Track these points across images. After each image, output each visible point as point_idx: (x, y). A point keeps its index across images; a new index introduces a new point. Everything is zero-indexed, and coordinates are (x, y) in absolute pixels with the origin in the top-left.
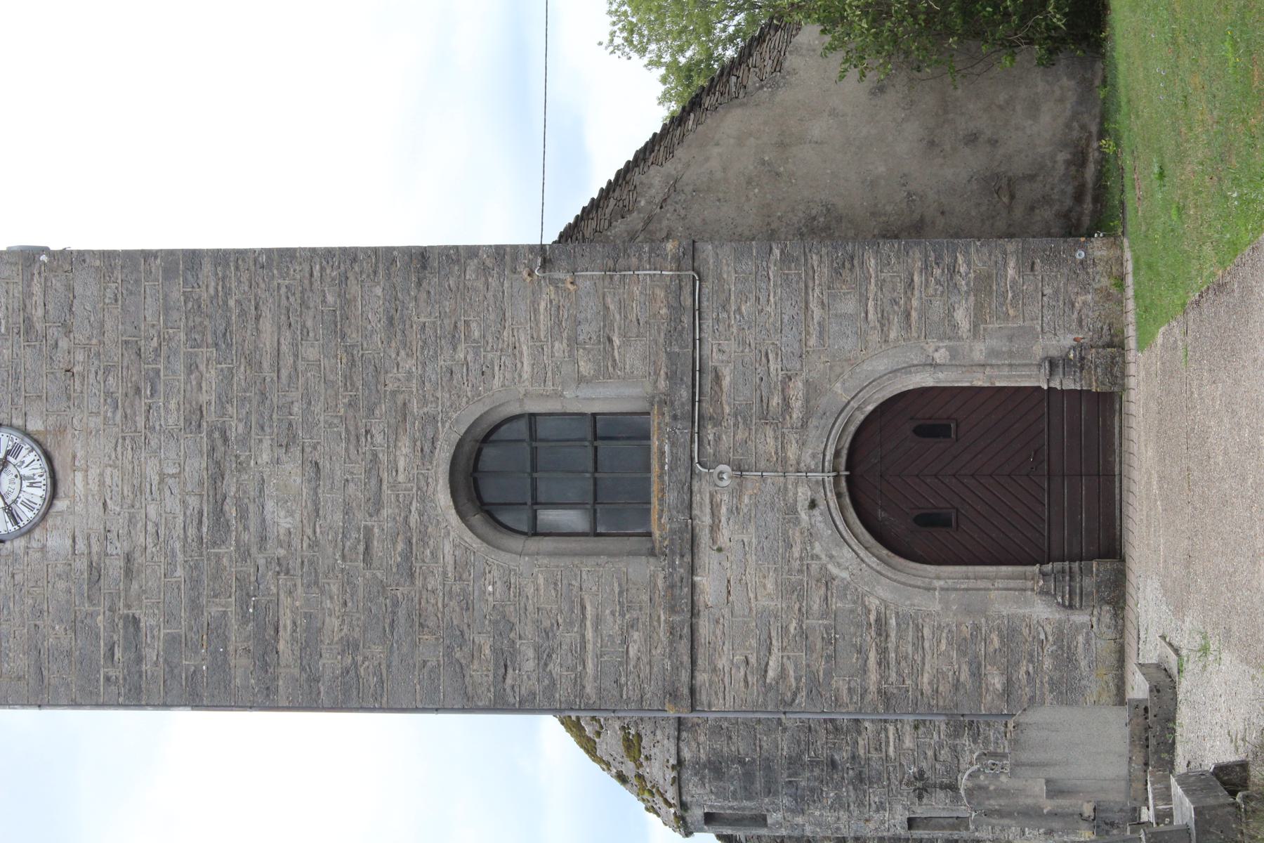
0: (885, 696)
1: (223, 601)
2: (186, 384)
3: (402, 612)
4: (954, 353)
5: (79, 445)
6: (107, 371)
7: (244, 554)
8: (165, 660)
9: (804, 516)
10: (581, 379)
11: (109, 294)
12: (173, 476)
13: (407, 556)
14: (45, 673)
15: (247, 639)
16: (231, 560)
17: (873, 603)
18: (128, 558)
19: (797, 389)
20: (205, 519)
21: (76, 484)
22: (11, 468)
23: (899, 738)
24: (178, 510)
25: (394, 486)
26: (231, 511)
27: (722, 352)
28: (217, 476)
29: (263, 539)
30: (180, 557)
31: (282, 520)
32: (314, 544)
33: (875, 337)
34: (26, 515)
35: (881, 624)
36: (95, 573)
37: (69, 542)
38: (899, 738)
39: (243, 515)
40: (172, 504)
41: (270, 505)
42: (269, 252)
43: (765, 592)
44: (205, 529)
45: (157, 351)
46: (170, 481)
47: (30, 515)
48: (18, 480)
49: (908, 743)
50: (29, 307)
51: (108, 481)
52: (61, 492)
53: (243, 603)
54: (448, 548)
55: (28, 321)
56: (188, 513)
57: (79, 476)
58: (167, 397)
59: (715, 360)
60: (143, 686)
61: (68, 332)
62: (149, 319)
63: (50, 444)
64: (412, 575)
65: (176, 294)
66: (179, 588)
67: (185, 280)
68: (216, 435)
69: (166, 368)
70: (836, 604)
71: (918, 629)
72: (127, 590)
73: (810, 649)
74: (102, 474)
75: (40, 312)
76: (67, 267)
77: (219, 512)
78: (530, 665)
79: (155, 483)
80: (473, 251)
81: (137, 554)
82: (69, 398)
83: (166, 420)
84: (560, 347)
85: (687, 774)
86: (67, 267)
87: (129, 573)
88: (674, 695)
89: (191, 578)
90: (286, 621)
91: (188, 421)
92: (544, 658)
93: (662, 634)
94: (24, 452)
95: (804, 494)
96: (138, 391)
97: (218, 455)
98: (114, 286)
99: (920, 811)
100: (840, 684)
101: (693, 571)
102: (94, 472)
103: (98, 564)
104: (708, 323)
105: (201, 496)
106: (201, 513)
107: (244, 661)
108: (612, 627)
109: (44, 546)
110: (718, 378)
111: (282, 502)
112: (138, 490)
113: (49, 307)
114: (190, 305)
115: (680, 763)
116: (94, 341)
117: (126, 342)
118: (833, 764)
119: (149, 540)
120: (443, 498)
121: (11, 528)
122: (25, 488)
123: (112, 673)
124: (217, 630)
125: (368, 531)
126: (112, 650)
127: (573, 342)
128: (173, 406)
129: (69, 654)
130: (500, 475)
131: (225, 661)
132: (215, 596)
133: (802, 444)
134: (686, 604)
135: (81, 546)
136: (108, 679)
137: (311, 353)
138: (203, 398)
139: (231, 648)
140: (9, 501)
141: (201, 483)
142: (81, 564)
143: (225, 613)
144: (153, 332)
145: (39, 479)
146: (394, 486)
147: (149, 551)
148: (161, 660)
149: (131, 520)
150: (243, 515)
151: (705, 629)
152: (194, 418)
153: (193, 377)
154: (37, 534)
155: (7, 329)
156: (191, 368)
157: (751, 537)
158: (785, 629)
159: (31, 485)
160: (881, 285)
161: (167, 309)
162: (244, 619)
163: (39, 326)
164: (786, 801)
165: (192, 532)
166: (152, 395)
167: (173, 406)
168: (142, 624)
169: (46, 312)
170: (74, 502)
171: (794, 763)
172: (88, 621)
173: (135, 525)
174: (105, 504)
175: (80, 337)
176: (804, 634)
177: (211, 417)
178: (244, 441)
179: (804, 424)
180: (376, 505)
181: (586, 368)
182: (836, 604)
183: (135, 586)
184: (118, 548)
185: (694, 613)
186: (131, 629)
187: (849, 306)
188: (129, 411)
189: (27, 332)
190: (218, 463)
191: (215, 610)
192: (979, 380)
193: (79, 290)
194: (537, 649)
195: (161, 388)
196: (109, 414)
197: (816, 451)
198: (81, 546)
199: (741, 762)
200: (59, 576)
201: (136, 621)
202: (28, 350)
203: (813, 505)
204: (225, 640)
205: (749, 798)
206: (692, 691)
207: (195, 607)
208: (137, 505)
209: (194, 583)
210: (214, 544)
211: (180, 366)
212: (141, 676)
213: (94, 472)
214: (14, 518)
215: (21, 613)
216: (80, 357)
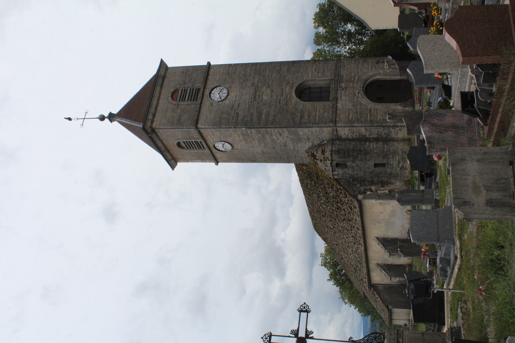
0: (371, 121)
3: (284, 111)
4: (384, 72)
7: (258, 103)
9: (357, 95)
10: (319, 77)
13: (286, 102)
17: (369, 107)
18: (239, 104)
19: (356, 77)
23: (373, 146)
25: (285, 93)
26: (257, 97)
27: (344, 73)
29: (262, 101)
31: (265, 98)
32: (271, 101)
33: (370, 70)
34: (223, 98)
35: (370, 110)
36: (233, 107)
38: (373, 146)
39: (259, 97)
40: (247, 97)
41: (264, 96)
42: (269, 62)
43: (350, 106)
49: (375, 146)
53: (257, 110)
54: (294, 101)
55: (229, 73)
59: (342, 73)
61: (234, 73)
64: (287, 105)
65: (253, 68)
70: (362, 107)
71: (377, 111)
73: (357, 114)
77: (255, 97)
78: (306, 118)
80: (303, 61)
84: (316, 73)
85: (333, 153)
87: (238, 106)
88: (332, 121)
90: (264, 112)
92: (309, 117)
93: (331, 112)
95: (357, 91)
99: (377, 162)
100: (363, 119)
101: (337, 103)
102: (235, 93)
104: (342, 69)
108: (322, 112)
110: (343, 76)
111: (266, 95)
112: (242, 95)
115: (332, 151)
118: (360, 150)
120: (294, 94)
124: (252, 114)
125: (280, 99)
127: (318, 72)
130: (304, 93)
133: (357, 85)
134: (335, 108)
135: (231, 103)
137: (274, 75)
142: (231, 105)
146: (285, 93)
150: (259, 97)
151: (338, 112)
152: (253, 84)
156: (254, 78)
157: (347, 98)
158: (353, 111)
160: (371, 63)
161: (251, 70)
162: (257, 112)
164: (351, 159)
171: (353, 150)
175: (236, 74)
176: (356, 112)
177: (256, 84)
178: (260, 87)
179: (358, 82)
180: (282, 95)
181: (320, 75)
182: (362, 107)
184: (237, 103)
185: (337, 109)
187: (366, 66)
191: (252, 111)
192: (388, 78)
194: (308, 115)
197: (358, 87)
198: (231, 103)
199: (343, 150)
201: (238, 113)
203: (359, 93)
205: (344, 158)
206: (336, 121)
207: (249, 111)
209: (249, 107)
211: (252, 78)
213: (235, 93)
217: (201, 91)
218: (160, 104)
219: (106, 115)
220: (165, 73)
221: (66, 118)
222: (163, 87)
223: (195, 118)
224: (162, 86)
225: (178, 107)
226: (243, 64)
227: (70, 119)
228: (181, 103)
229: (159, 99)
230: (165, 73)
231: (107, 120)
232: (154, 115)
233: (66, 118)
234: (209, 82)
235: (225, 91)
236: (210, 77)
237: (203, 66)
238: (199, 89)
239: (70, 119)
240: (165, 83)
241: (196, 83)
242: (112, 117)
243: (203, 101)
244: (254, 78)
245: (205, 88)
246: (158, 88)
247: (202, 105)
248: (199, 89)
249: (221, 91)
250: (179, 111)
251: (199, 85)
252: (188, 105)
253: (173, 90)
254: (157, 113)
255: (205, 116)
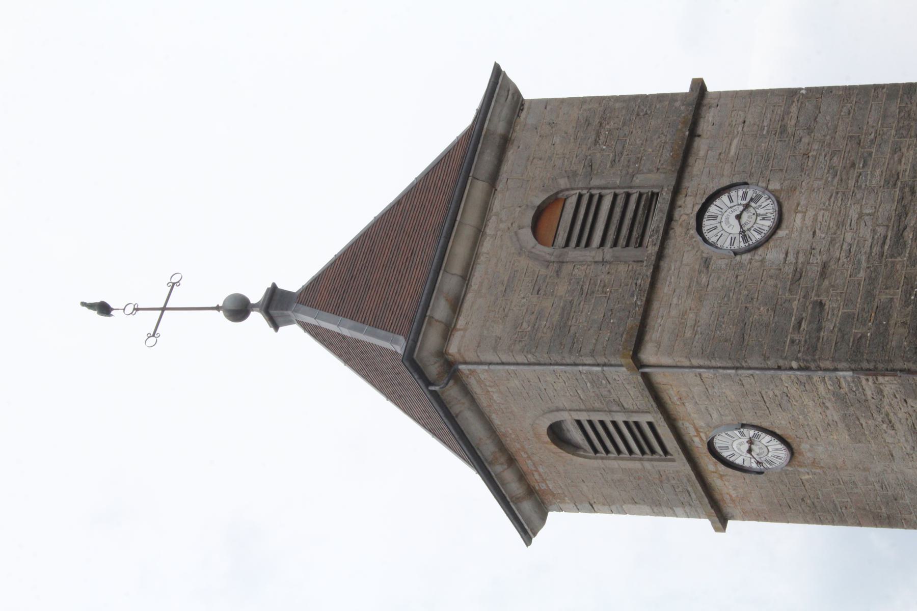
1: (892, 291)
2: (890, 159)
5: (803, 198)
6: (833, 154)
8: (840, 329)
11: (845, 110)
12: (869, 214)
14: (746, 337)
15: (907, 315)
16: (903, 266)
18: (825, 266)
20: (888, 241)
21: (795, 221)
22: (751, 210)
24: (869, 236)
28: (903, 214)
30: (864, 264)
34: (756, 237)
36: (798, 275)
37: (782, 256)
44: (886, 247)
45: (872, 142)
46: (866, 218)
47: (758, 237)
48: (754, 217)
50: (786, 119)
51: (820, 218)
52: (784, 225)
53: (907, 293)
55: (784, 129)
56: (876, 237)
57: (799, 216)
58: (874, 167)
60: (819, 345)
61: (810, 130)
62: (870, 123)
63: (783, 196)
65: (894, 108)
66: (859, 284)
67: (902, 100)
68: (907, 190)
69: (877, 151)
72: (819, 285)
74: (816, 215)
75: (793, 122)
76: (818, 95)
77: (899, 235)
79: (854, 219)
81: (832, 263)
82: (802, 171)
83: (871, 181)
86: (818, 95)
87: (823, 274)
89: (870, 278)
91: (887, 182)
94: (763, 199)
96: (853, 165)
97: (905, 202)
98: (849, 105)
102: (811, 213)
103: (801, 270)
105: (888, 226)
106: (885, 237)
107: (901, 330)
109: (764, 258)
112: (840, 224)
113: (801, 119)
114: (902, 114)
116: (828, 137)
117: (851, 137)
119: (843, 254)
121: (742, 245)
122: (758, 221)
123: (796, 337)
124: (884, 311)
126: (800, 323)
128: (878, 172)
129: (767, 325)
131: (886, 330)
132: (886, 288)
135: (791, 258)
136: (793, 341)
138: (901, 168)
139: (892, 322)
140: (745, 228)
141: (889, 219)
143: (892, 299)
144: (871, 130)
145: (769, 215)
147: (841, 261)
148: (836, 330)
149: (832, 241)
152: (892, 180)
153: (896, 156)
154: (760, 251)
155: (768, 132)
156: (896, 149)
159: (763, 219)
161: (885, 117)
162: (906, 303)
163: (790, 130)
165: (876, 249)
166: (863, 166)
167: (878, 172)
168: (826, 307)
169: (798, 121)
170: (792, 232)
172: (786, 305)
173: (834, 245)
174: (814, 233)
183: (826, 283)
184: (817, 259)
186: (818, 310)
188: (844, 177)
189: (781, 133)
190: (904, 207)
191: (884, 297)
193: (823, 108)
195: (871, 163)
196: (830, 179)
198: (791, 258)
200: (771, 277)
201: (821, 305)
202: (780, 143)
204: (888, 317)
207: (870, 295)
208: (839, 232)
209: (872, 280)
210: (892, 256)
211: (887, 149)
212: (818, 340)
213: (811, 213)
214: (745, 238)
215: (738, 300)
216: (816, 146)
217: (662, 204)
218: (482, 258)
219: (256, 296)
220: (511, 124)
221: (91, 306)
222: (500, 186)
223: (633, 322)
224: (493, 179)
225: (558, 273)
226: (849, 90)
227: (104, 309)
228: (573, 254)
229: (479, 233)
230: (511, 124)
231: (256, 318)
232: (456, 305)
233: (91, 306)
234: (697, 167)
235: (767, 207)
236: (701, 146)
237: (673, 97)
238: (654, 196)
239: (104, 309)
240: (506, 168)
241: (639, 171)
242: (277, 306)
243: (669, 251)
244: (896, 149)
245: (677, 191)
246: (478, 189)
247: (664, 264)
248: (654, 196)
249: (747, 206)
250: (562, 289)
251: (653, 178)
252: (604, 262)
253: (538, 202)
254: (470, 297)
255: (674, 312)
